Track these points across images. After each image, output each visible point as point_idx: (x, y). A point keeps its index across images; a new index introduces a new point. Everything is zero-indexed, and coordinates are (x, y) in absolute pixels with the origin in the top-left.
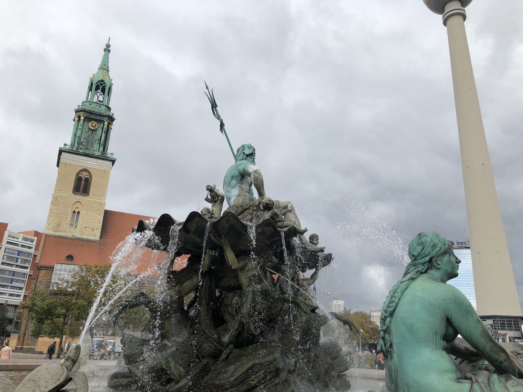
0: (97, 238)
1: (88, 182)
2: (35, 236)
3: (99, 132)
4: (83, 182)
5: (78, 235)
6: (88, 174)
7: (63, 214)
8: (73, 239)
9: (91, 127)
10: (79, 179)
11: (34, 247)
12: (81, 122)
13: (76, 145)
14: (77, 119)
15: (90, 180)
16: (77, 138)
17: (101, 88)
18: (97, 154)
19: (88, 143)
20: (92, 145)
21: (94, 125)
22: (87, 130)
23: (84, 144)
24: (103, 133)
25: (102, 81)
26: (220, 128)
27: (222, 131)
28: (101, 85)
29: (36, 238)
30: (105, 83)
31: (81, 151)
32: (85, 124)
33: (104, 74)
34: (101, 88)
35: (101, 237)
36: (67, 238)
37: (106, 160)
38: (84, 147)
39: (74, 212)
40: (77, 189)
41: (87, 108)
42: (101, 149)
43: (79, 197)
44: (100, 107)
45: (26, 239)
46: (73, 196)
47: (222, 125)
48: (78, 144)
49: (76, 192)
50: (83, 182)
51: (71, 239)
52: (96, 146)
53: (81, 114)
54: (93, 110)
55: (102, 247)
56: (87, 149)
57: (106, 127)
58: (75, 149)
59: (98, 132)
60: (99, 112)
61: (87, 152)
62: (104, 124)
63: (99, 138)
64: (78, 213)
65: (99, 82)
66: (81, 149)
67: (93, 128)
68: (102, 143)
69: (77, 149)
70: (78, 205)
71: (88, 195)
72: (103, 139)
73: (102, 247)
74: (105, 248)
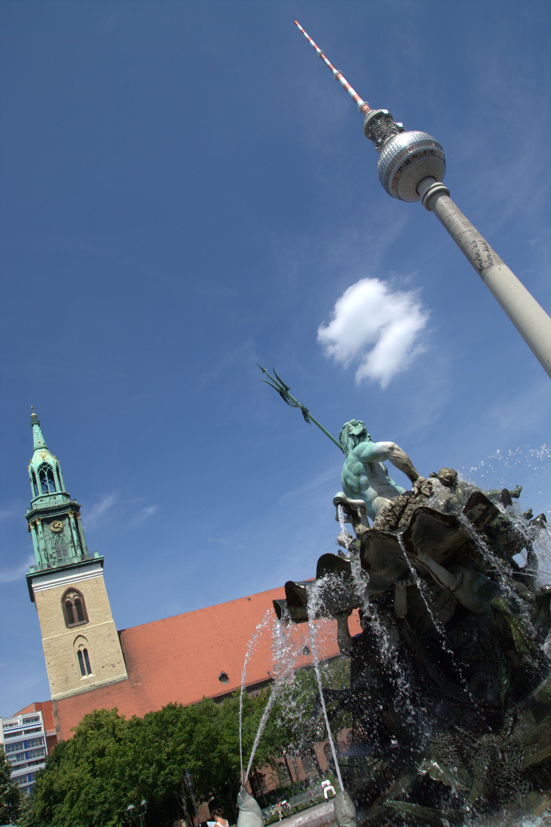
0: (125, 674)
1: (80, 604)
2: (37, 710)
3: (67, 531)
4: (74, 607)
5: (97, 683)
6: (75, 593)
7: (66, 662)
8: (93, 690)
9: (55, 530)
10: (67, 606)
11: (42, 726)
12: (40, 528)
13: (45, 561)
14: (32, 527)
15: (81, 600)
16: (42, 553)
17: (46, 473)
18: (76, 561)
19: (58, 552)
20: (65, 553)
21: (56, 525)
22: (51, 536)
23: (55, 555)
24: (73, 530)
25: (45, 464)
26: (303, 416)
27: (307, 421)
28: (45, 469)
29: (39, 713)
30: (49, 466)
31: (55, 567)
32: (45, 529)
33: (43, 454)
34: (46, 473)
35: (128, 671)
36: (86, 693)
37: (92, 564)
38: (57, 560)
39: (79, 653)
40: (70, 621)
41: (39, 508)
42: (79, 552)
43: (77, 631)
44: (55, 498)
45: (26, 721)
46: (69, 631)
47: (305, 413)
48: (47, 559)
49: (70, 625)
50: (74, 607)
51: (89, 692)
52: (71, 552)
53: (35, 518)
54: (48, 506)
55: (136, 684)
56: (60, 560)
57: (72, 520)
58: (45, 568)
59: (66, 532)
60: (57, 505)
61: (63, 564)
62: (69, 519)
63: (70, 539)
64: (85, 651)
65: (40, 467)
66: (54, 564)
67: (57, 530)
68: (76, 544)
69: (49, 566)
70: (80, 641)
71: (88, 621)
72: (76, 538)
73: (136, 684)
74: (140, 684)
